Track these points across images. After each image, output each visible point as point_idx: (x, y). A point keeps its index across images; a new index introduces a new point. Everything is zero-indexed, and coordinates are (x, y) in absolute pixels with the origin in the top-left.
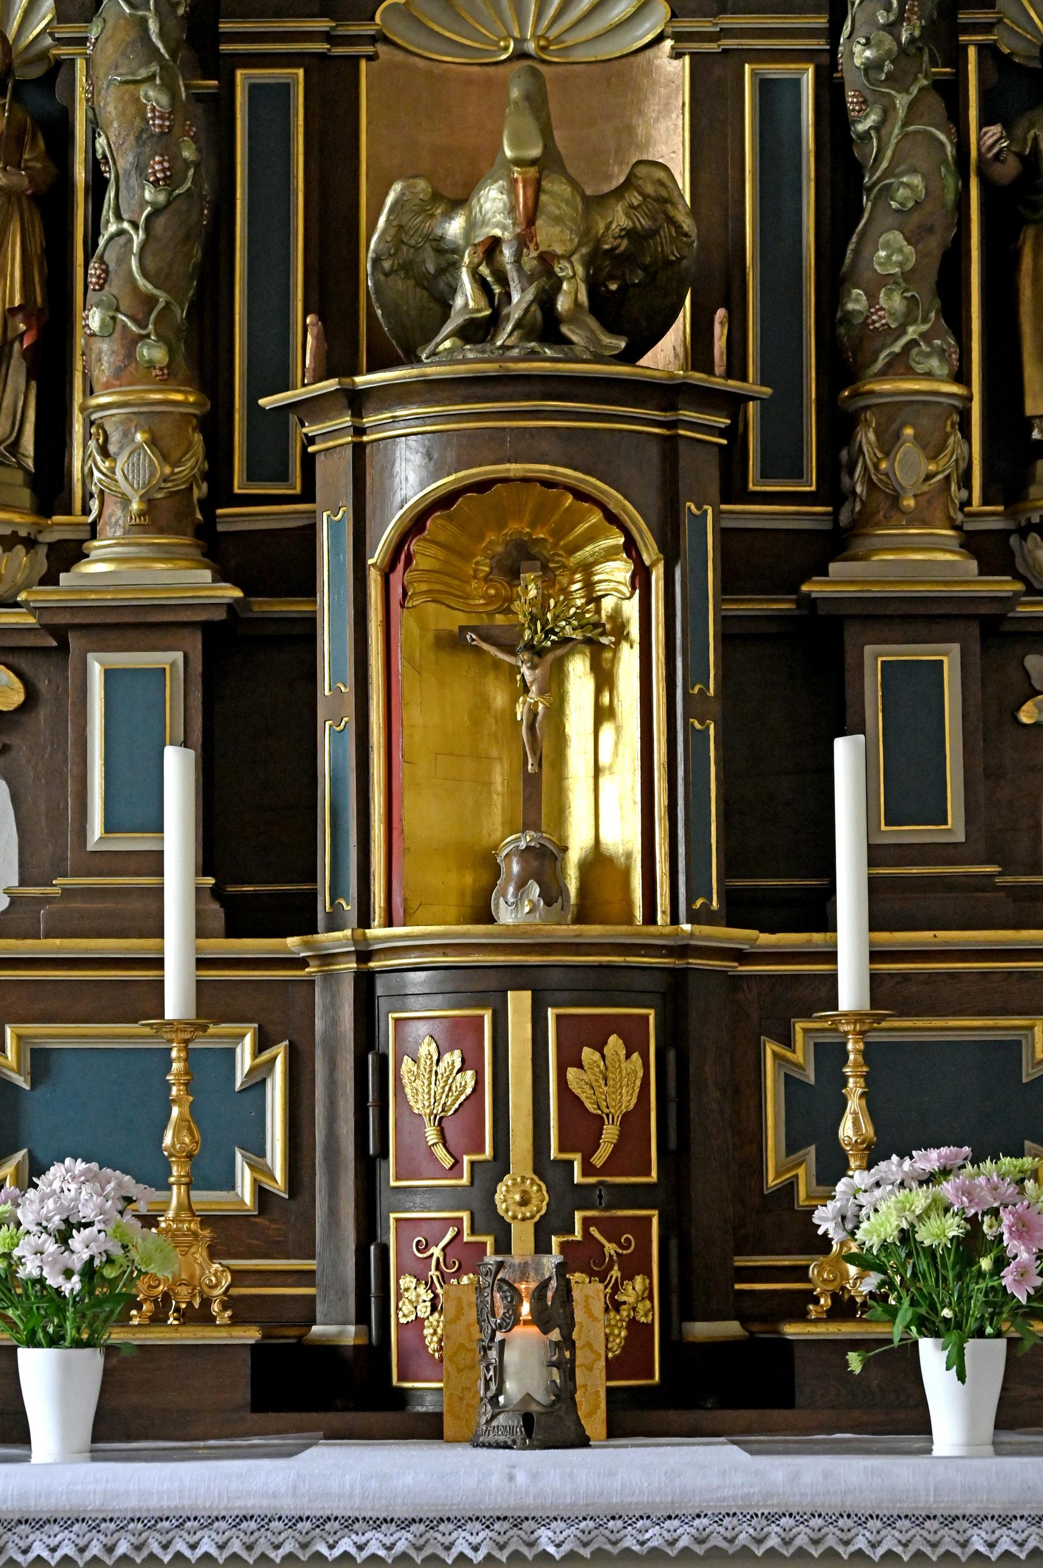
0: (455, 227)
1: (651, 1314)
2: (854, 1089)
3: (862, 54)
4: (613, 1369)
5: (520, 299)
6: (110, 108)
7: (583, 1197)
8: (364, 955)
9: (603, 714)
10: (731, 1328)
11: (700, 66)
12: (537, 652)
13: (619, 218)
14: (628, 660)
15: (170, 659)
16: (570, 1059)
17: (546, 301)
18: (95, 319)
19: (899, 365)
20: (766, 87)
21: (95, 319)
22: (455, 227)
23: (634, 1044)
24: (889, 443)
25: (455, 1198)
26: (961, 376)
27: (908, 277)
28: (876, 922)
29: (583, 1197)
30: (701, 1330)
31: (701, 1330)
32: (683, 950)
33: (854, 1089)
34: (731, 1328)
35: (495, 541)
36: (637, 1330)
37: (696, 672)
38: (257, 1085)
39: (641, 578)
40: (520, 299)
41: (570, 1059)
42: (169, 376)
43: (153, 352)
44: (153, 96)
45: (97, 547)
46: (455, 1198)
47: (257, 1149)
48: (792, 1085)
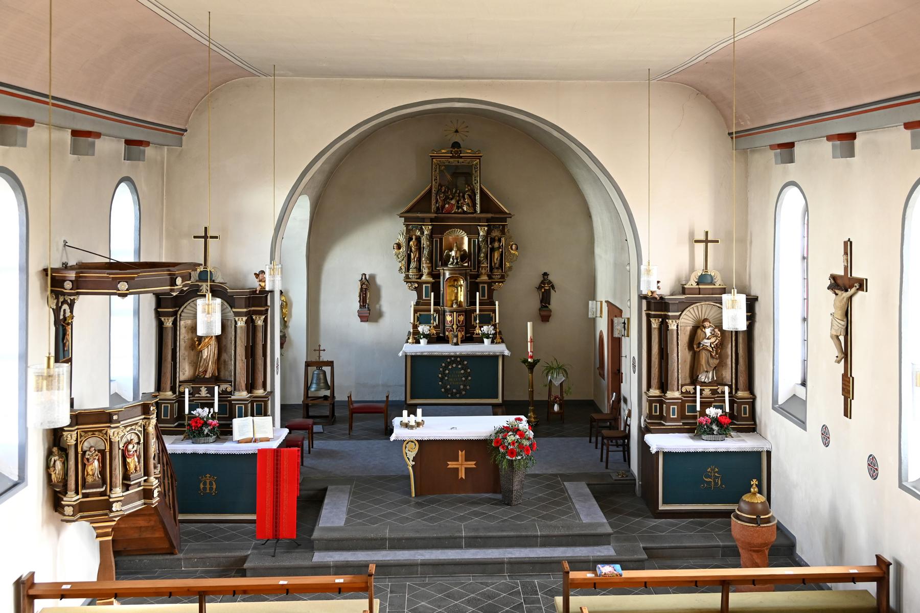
0: (450, 253)
1: (464, 334)
2: (478, 319)
3: (481, 240)
4: (461, 338)
5: (455, 261)
6: (425, 243)
7: (459, 326)
8: (444, 309)
9: (461, 291)
10: (469, 335)
11: (469, 239)
12: (456, 287)
13: (462, 253)
14: (463, 288)
15: (429, 285)
16: (458, 317)
17: (457, 261)
18: (424, 259)
19: (483, 264)
20: (473, 240)
21: (424, 259)
22: (450, 253)
23: (463, 315)
24: (482, 270)
25: (450, 326)
26: (488, 264)
27: (484, 257)
28: (480, 305)
29: (459, 326)
30: (468, 335)
31: (468, 335)
32: (466, 309)
33: (478, 319)
34: (469, 335)
35: (453, 279)
36: (463, 336)
37: (467, 288)
38: (436, 316)
39: (464, 282)
40: (455, 261)
41: (458, 317)
42: (429, 264)
43: (428, 262)
44: (428, 243)
45: (424, 276)
46: (450, 326)
47: (436, 321)
48: (474, 317)
